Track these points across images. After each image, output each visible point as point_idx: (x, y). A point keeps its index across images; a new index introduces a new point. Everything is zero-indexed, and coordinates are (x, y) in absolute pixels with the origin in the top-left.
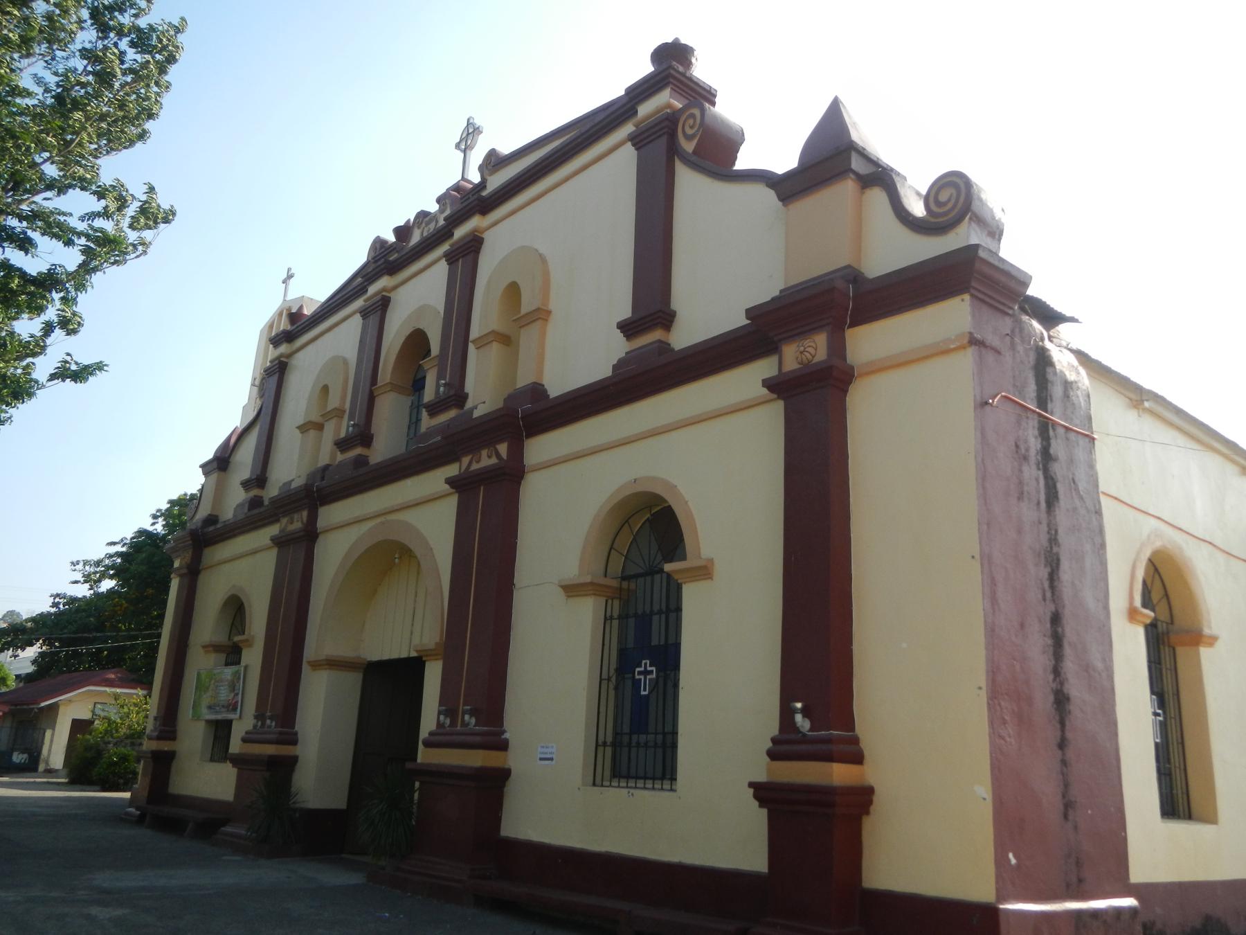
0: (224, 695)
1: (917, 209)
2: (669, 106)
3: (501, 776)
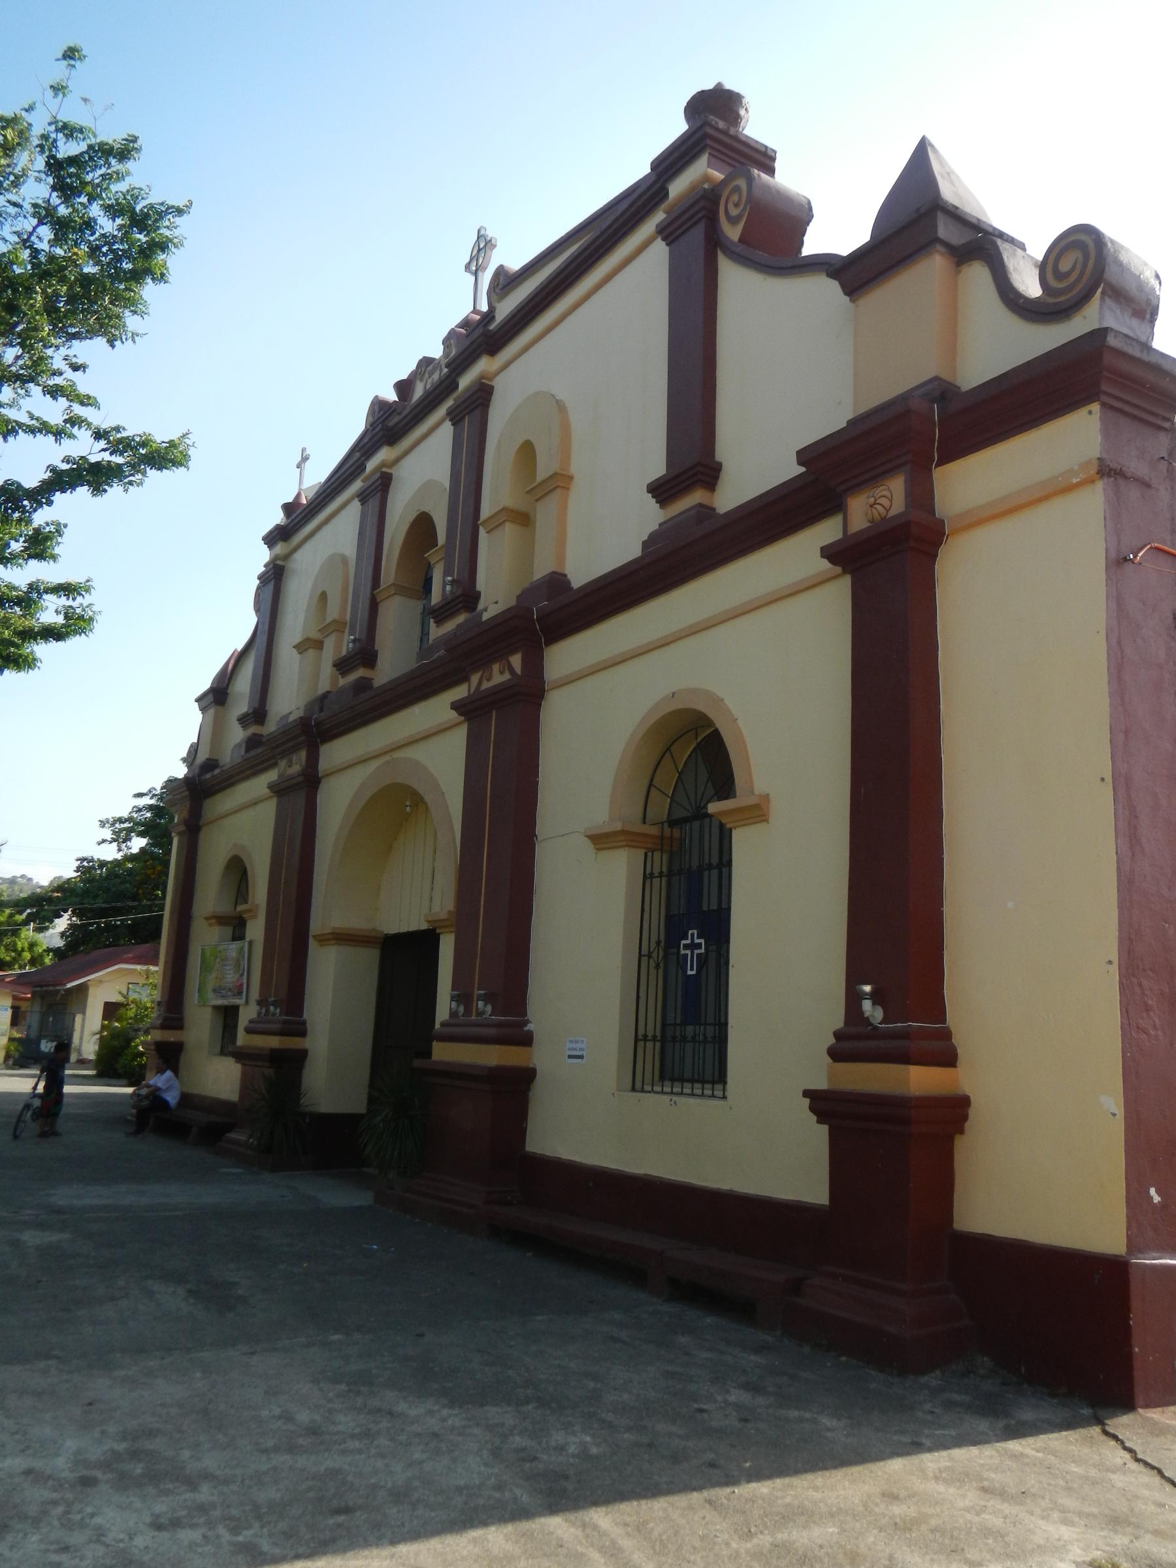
0: (231, 977)
1: (1030, 286)
2: (706, 178)
3: (525, 1078)
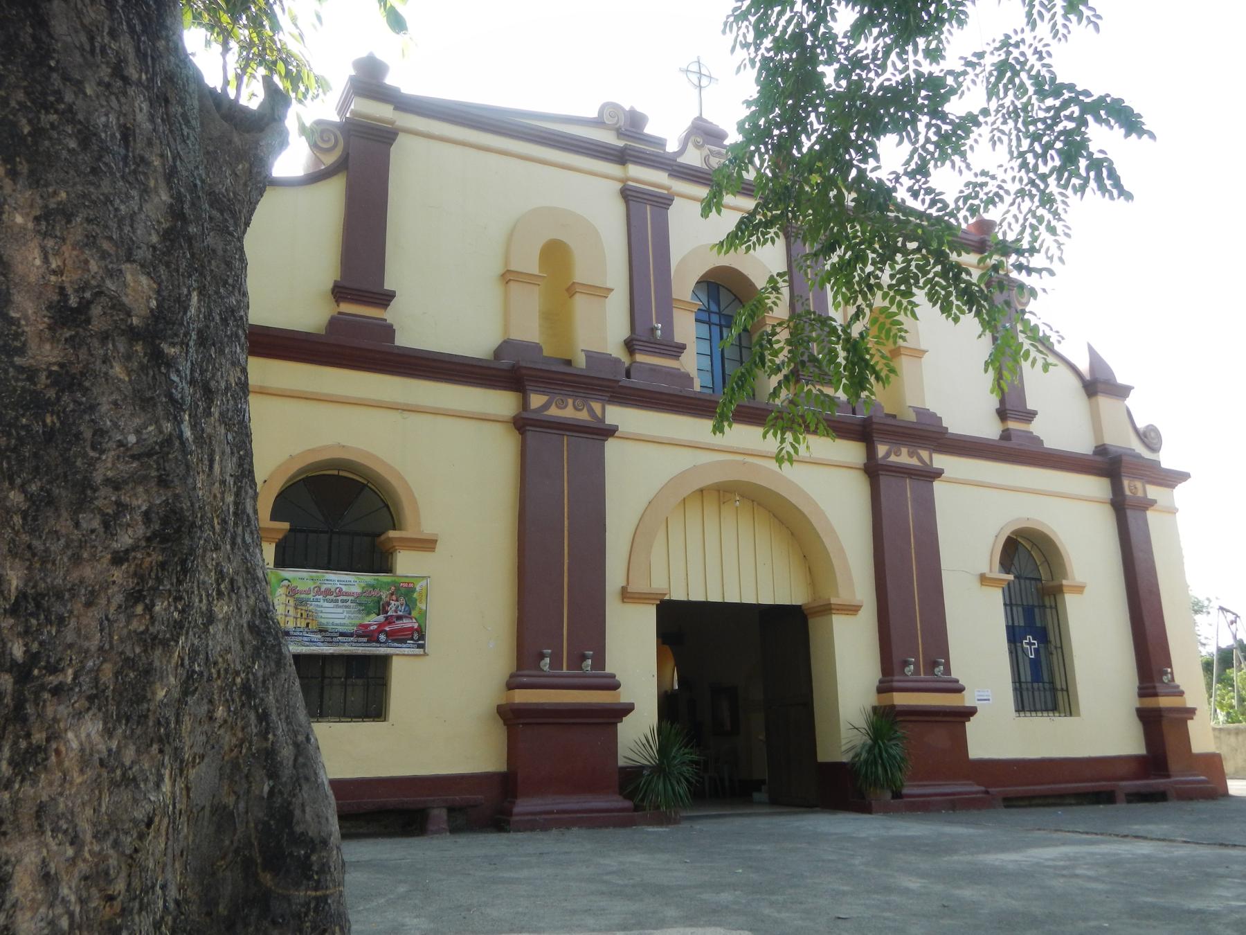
0: (338, 616)
